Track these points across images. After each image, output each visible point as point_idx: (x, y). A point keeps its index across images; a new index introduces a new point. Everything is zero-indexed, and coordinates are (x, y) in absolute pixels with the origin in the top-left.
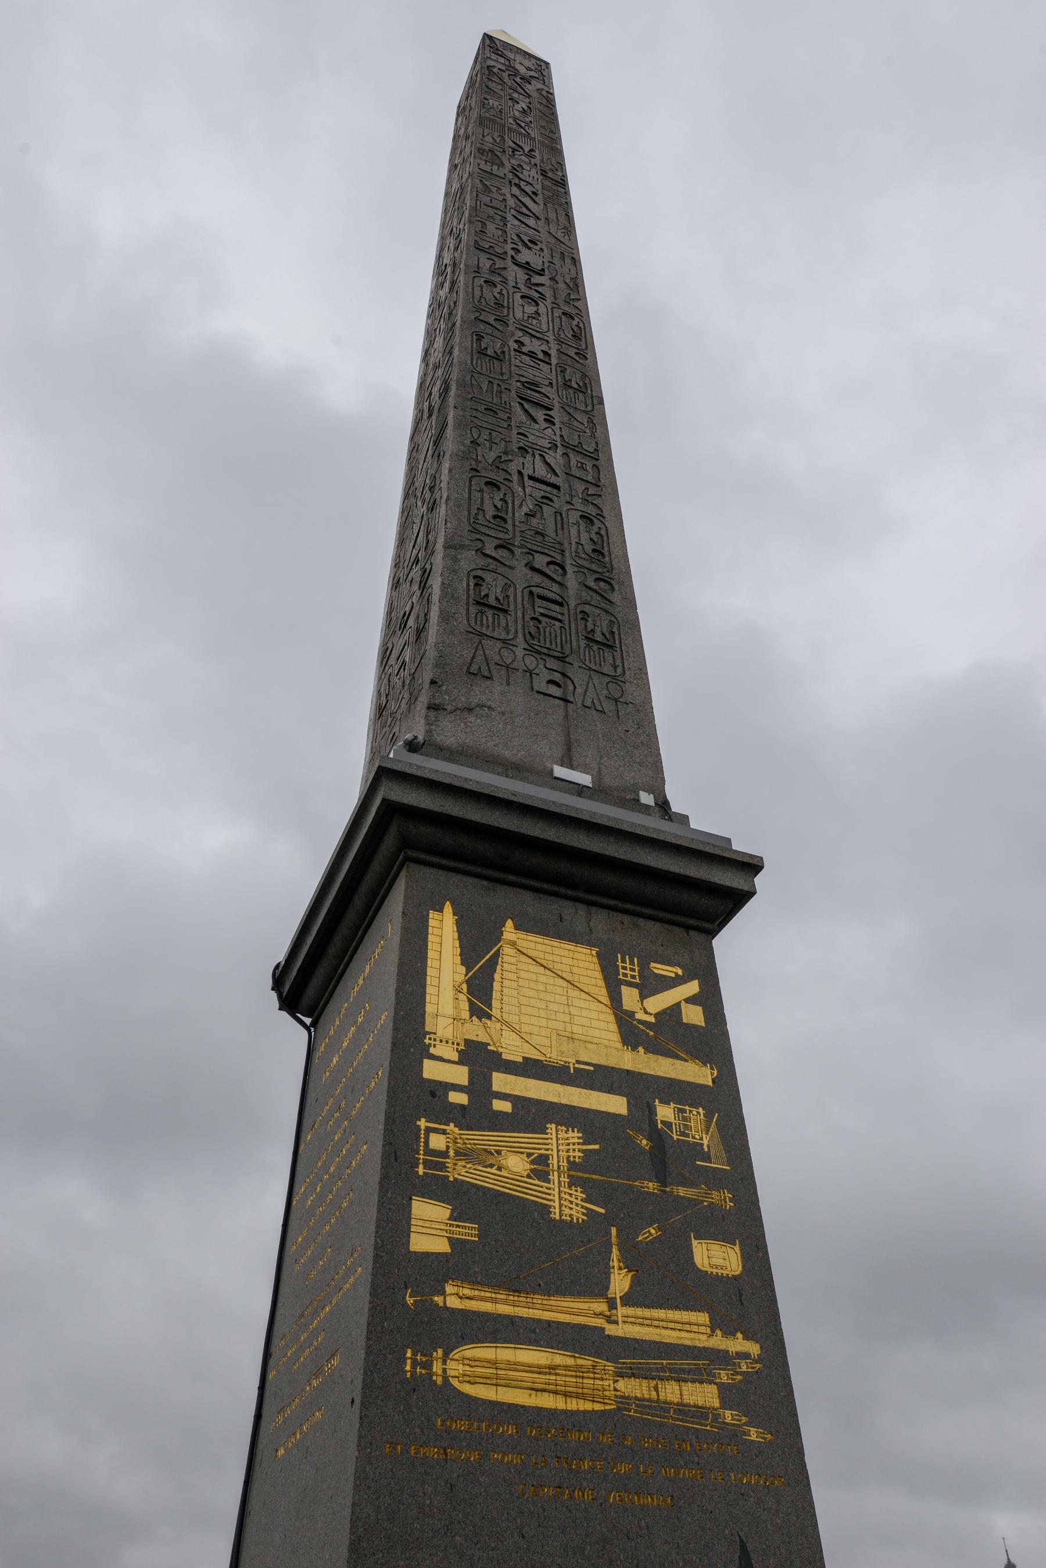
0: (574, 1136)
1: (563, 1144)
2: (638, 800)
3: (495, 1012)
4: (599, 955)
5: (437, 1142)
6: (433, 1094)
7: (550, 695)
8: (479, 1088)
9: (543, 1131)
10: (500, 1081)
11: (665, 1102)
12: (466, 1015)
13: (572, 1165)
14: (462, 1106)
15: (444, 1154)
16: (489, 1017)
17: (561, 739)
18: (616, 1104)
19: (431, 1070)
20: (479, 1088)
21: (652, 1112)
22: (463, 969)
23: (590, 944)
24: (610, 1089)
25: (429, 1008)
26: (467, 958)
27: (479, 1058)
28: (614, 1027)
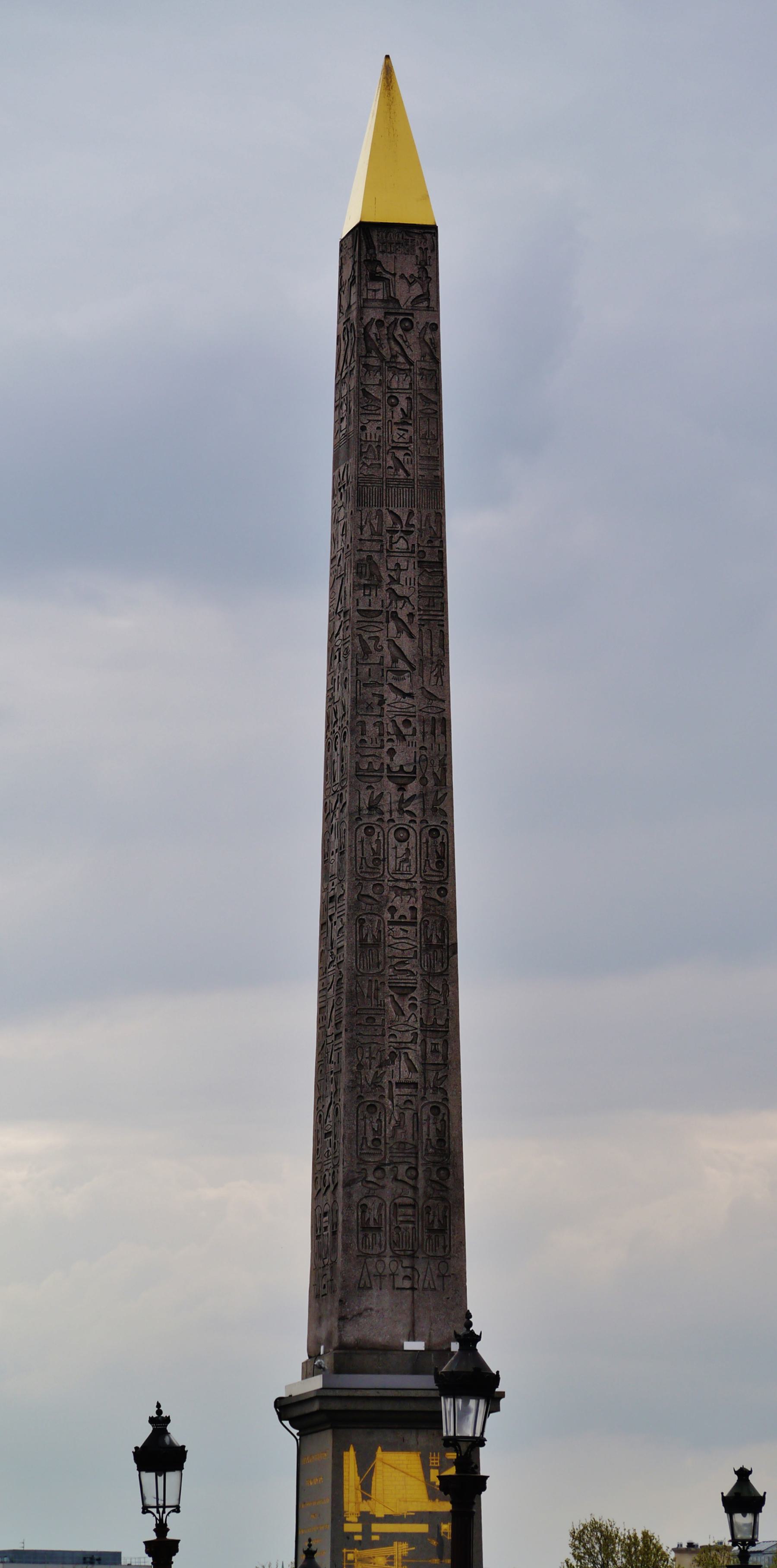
0: (405, 1545)
1: (401, 1549)
2: (449, 1349)
3: (373, 1496)
4: (421, 1456)
5: (350, 1557)
6: (348, 1538)
7: (404, 1289)
8: (367, 1532)
9: (392, 1545)
10: (376, 1527)
11: (445, 1523)
12: (360, 1500)
13: (403, 1557)
14: (360, 1541)
15: (353, 1561)
16: (370, 1499)
17: (409, 1320)
18: (423, 1528)
19: (348, 1528)
20: (367, 1532)
21: (439, 1528)
22: (358, 1478)
23: (417, 1450)
24: (421, 1522)
25: (345, 1500)
26: (360, 1473)
27: (366, 1519)
28: (425, 1491)
